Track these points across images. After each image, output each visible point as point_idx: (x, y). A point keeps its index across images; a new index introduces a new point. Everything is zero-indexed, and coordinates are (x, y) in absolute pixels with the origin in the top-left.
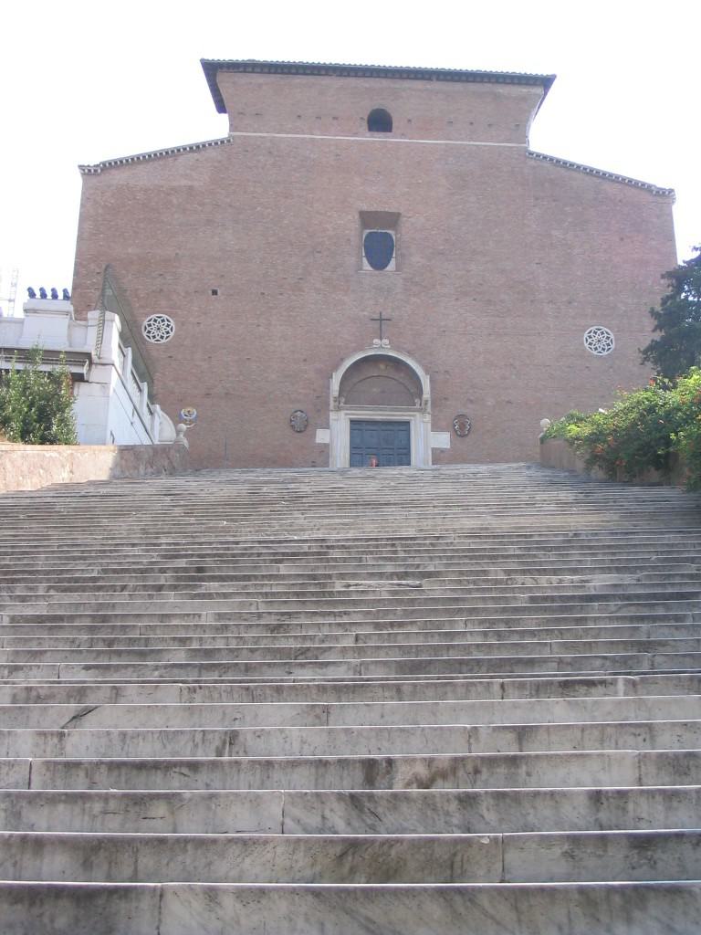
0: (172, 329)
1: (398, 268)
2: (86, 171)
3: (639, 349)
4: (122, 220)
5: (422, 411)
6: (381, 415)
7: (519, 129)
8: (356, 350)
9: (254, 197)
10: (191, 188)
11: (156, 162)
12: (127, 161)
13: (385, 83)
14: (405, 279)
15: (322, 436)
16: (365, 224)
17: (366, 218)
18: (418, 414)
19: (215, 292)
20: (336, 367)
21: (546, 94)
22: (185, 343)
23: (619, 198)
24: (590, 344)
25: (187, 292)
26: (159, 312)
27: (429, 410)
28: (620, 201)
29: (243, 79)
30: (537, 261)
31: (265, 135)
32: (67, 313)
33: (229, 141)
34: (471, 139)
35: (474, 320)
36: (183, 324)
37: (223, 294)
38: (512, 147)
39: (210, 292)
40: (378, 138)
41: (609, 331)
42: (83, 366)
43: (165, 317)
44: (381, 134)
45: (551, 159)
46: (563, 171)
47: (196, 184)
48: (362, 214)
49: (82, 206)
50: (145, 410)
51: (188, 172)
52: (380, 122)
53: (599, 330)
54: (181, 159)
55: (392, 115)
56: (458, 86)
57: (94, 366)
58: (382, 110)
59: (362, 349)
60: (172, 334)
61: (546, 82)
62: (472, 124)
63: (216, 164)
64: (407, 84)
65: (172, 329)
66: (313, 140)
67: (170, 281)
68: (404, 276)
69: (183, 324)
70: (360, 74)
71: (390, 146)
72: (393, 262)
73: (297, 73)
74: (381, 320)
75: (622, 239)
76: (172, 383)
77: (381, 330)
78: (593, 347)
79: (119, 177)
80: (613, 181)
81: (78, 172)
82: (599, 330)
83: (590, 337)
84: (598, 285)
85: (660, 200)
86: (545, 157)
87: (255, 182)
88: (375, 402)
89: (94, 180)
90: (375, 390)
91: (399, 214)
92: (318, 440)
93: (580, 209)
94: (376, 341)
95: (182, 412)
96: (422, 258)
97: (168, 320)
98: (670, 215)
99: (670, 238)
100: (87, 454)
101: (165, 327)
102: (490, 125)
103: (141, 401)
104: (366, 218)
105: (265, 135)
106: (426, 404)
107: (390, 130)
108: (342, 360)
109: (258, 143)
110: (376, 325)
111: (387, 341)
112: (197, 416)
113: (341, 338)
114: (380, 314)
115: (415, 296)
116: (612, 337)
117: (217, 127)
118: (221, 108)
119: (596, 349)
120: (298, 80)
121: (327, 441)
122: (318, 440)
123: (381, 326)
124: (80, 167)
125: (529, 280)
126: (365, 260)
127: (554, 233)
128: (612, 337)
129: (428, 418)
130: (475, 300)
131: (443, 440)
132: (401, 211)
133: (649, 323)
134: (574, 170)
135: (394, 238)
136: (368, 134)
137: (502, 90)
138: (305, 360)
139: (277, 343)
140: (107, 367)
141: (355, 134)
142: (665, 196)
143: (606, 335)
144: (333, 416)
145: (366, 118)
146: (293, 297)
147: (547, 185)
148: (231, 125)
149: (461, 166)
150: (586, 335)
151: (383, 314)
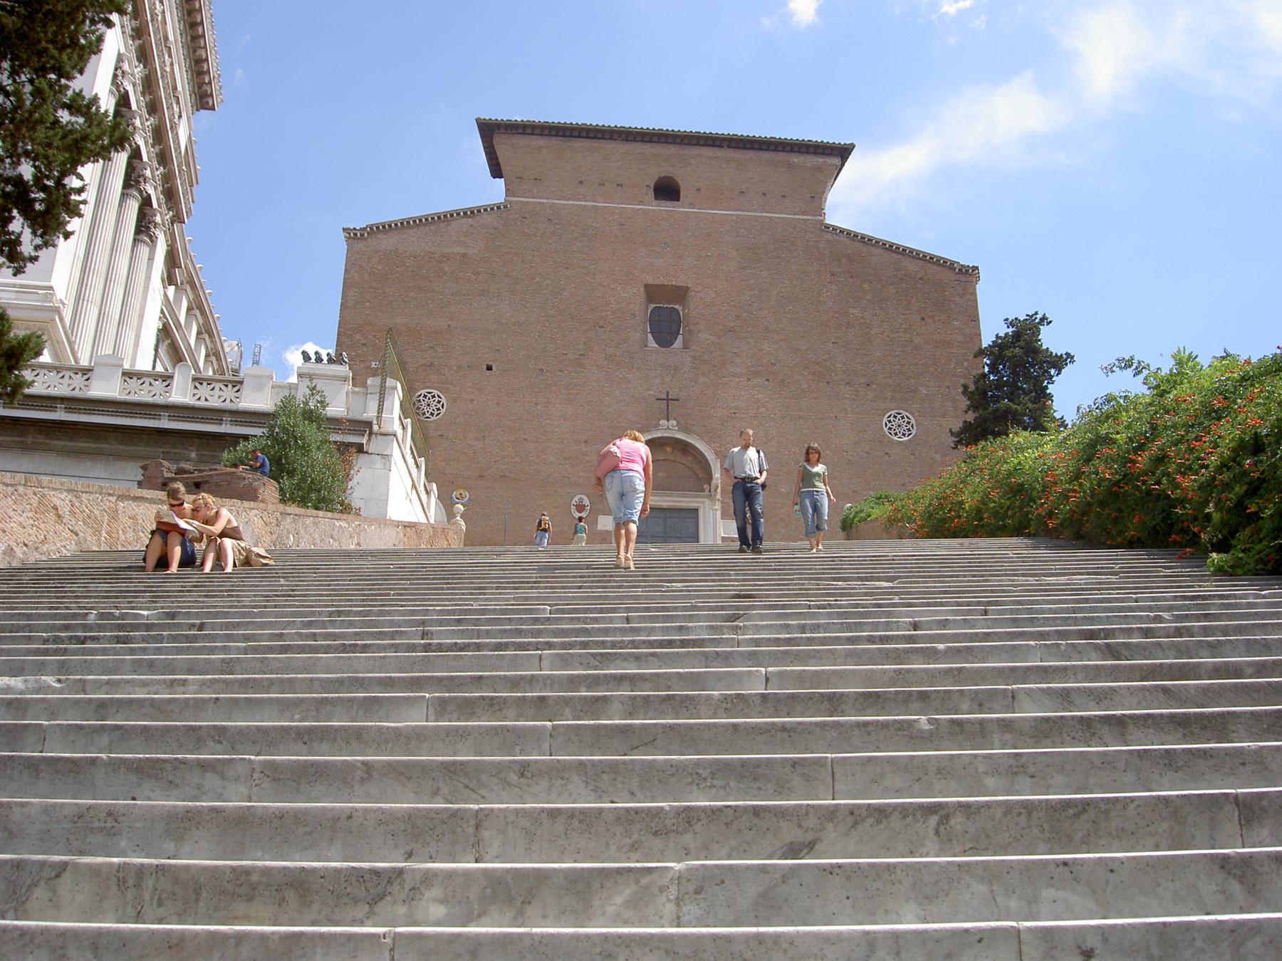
0: (443, 406)
1: (686, 346)
2: (352, 234)
3: (951, 431)
4: (390, 287)
5: (711, 496)
6: (667, 501)
7: (816, 200)
9: (532, 267)
10: (465, 255)
11: (427, 228)
12: (396, 225)
13: (672, 149)
14: (692, 357)
16: (650, 299)
17: (652, 292)
18: (707, 501)
19: (489, 368)
21: (843, 165)
22: (457, 421)
23: (918, 277)
24: (890, 429)
25: (459, 367)
26: (429, 388)
27: (719, 496)
28: (921, 279)
29: (523, 141)
30: (833, 340)
31: (545, 201)
32: (345, 379)
33: (506, 207)
34: (764, 210)
35: (767, 402)
36: (455, 400)
37: (498, 369)
38: (808, 220)
39: (485, 367)
40: (665, 207)
41: (909, 416)
42: (364, 435)
43: (436, 392)
44: (669, 203)
45: (849, 233)
46: (860, 246)
47: (470, 251)
48: (647, 287)
49: (346, 271)
50: (422, 488)
51: (462, 238)
52: (667, 190)
53: (899, 414)
54: (453, 225)
55: (680, 182)
56: (750, 155)
57: (374, 436)
58: (670, 177)
60: (443, 411)
61: (843, 152)
62: (764, 194)
63: (493, 231)
64: (696, 151)
65: (443, 406)
66: (595, 209)
67: (442, 355)
68: (692, 354)
69: (455, 400)
70: (647, 138)
71: (677, 216)
72: (680, 337)
73: (579, 136)
74: (668, 400)
75: (923, 319)
76: (443, 464)
77: (668, 409)
78: (892, 432)
79: (386, 242)
80: (913, 257)
81: (342, 235)
82: (899, 414)
83: (890, 421)
84: (898, 367)
85: (962, 278)
86: (842, 231)
87: (533, 250)
89: (361, 245)
90: (661, 474)
91: (687, 289)
92: (600, 527)
93: (879, 285)
94: (663, 422)
95: (454, 496)
96: (710, 335)
97: (439, 397)
98: (974, 294)
99: (974, 319)
100: (373, 527)
101: (435, 403)
102: (784, 196)
103: (419, 478)
104: (652, 292)
105: (545, 201)
106: (716, 490)
107: (678, 199)
109: (538, 209)
110: (663, 404)
111: (675, 423)
112: (469, 499)
113: (625, 419)
114: (668, 392)
115: (703, 374)
116: (913, 421)
117: (495, 191)
118: (496, 172)
119: (896, 434)
120: (580, 144)
122: (600, 527)
123: (668, 406)
124: (344, 230)
125: (825, 360)
126: (649, 335)
127: (852, 311)
128: (913, 421)
129: (718, 506)
130: (767, 380)
132: (689, 286)
133: (964, 402)
134: (872, 245)
135: (681, 313)
136: (655, 202)
137: (796, 159)
138: (586, 442)
139: (555, 423)
140: (388, 437)
141: (642, 203)
142: (968, 274)
143: (906, 419)
145: (652, 186)
146: (573, 374)
147: (843, 260)
148: (507, 190)
149: (754, 238)
150: (885, 420)
151: (671, 392)
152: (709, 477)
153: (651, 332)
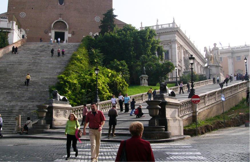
5: (67, 30)
8: (56, 20)
14: (65, 7)
15: (50, 34)
20: (53, 23)
59: (57, 19)
72: (63, 3)
88: (59, 29)
90: (59, 27)
94: (60, 18)
108: (54, 21)
121: (51, 35)
126: (59, 3)
129: (68, 32)
131: (70, 35)
144: (52, 31)
152: (67, 27)
153: (59, 2)
